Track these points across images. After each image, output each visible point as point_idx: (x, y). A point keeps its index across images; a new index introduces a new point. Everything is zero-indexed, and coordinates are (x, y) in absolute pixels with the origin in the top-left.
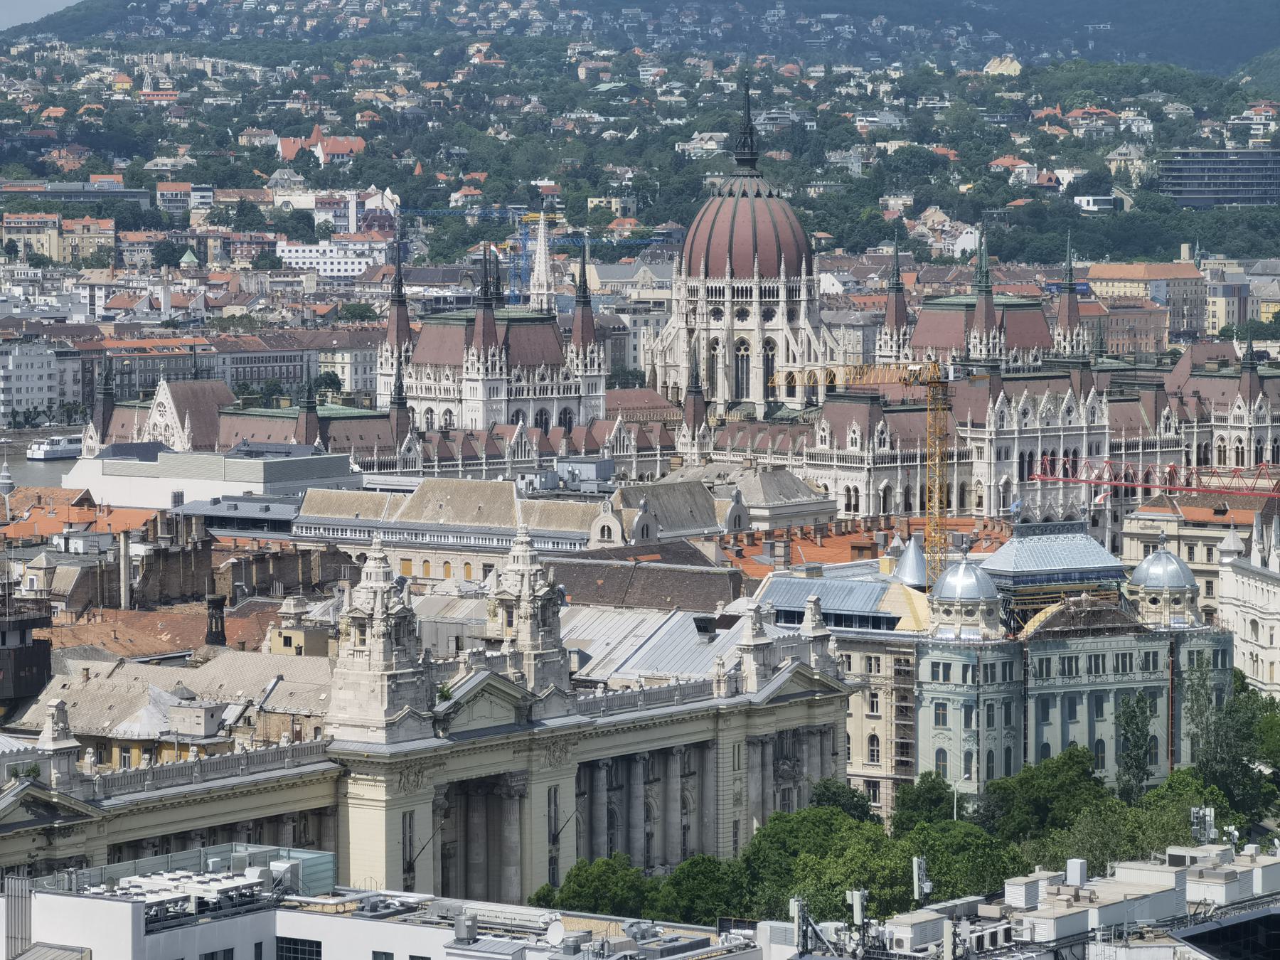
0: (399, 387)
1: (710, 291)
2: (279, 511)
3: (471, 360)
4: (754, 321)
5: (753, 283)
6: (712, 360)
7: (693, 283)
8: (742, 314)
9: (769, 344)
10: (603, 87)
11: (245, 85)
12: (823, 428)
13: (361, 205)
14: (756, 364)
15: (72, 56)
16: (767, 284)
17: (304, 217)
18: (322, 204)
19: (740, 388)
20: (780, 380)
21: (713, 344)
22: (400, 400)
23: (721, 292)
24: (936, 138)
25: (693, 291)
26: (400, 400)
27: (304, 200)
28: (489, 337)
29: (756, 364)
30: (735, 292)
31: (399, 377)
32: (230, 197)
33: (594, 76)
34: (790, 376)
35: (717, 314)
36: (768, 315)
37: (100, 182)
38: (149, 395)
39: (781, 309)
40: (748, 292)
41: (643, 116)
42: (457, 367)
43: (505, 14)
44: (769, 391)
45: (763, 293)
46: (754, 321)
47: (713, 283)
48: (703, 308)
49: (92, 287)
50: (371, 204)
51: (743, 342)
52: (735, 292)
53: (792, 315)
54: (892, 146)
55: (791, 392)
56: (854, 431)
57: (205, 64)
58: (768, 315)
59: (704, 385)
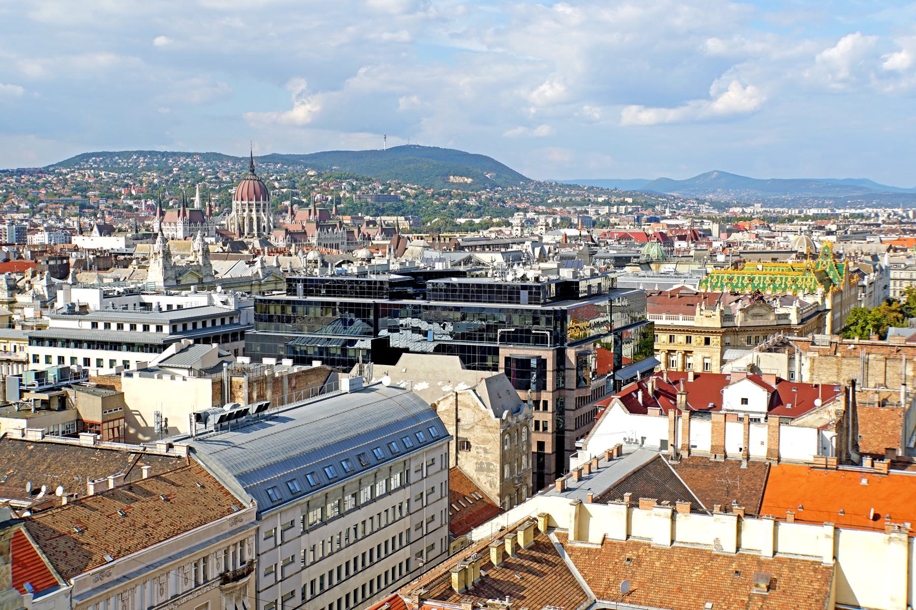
0: (160, 226)
2: (130, 250)
7: (238, 202)
9: (258, 218)
10: (209, 177)
11: (113, 176)
12: (273, 238)
13: (145, 203)
15: (64, 171)
17: (131, 207)
19: (251, 229)
24: (296, 188)
25: (237, 205)
26: (161, 230)
27: (131, 203)
28: (184, 214)
29: (255, 223)
31: (160, 226)
32: (111, 202)
33: (206, 175)
36: (258, 211)
37: (74, 198)
38: (92, 230)
41: (221, 182)
42: (175, 223)
43: (182, 163)
45: (256, 205)
46: (254, 213)
47: (243, 202)
50: (148, 203)
54: (285, 190)
55: (264, 231)
56: (281, 238)
57: (102, 173)
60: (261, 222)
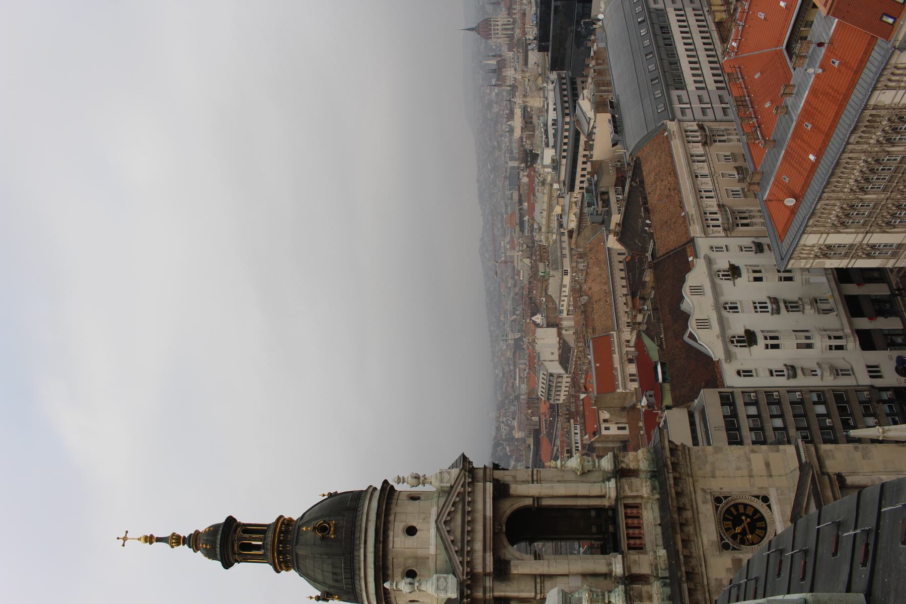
0: (507, 86)
1: (494, 35)
3: (504, 74)
4: (499, 27)
5: (492, 27)
6: (505, 34)
8: (498, 29)
14: (505, 27)
16: (493, 25)
18: (494, 91)
19: (508, 29)
20: (509, 22)
21: (502, 34)
22: (510, 86)
23: (494, 33)
25: (494, 38)
26: (510, 86)
27: (494, 94)
29: (505, 27)
30: (494, 31)
34: (508, 21)
35: (498, 33)
36: (498, 25)
39: (496, 23)
40: (494, 28)
42: (506, 76)
44: (509, 25)
46: (499, 27)
48: (497, 36)
49: (505, 128)
51: (502, 29)
52: (494, 31)
53: (498, 21)
55: (510, 21)
56: (514, 11)
58: (498, 25)
59: (509, 35)
60: (505, 23)
